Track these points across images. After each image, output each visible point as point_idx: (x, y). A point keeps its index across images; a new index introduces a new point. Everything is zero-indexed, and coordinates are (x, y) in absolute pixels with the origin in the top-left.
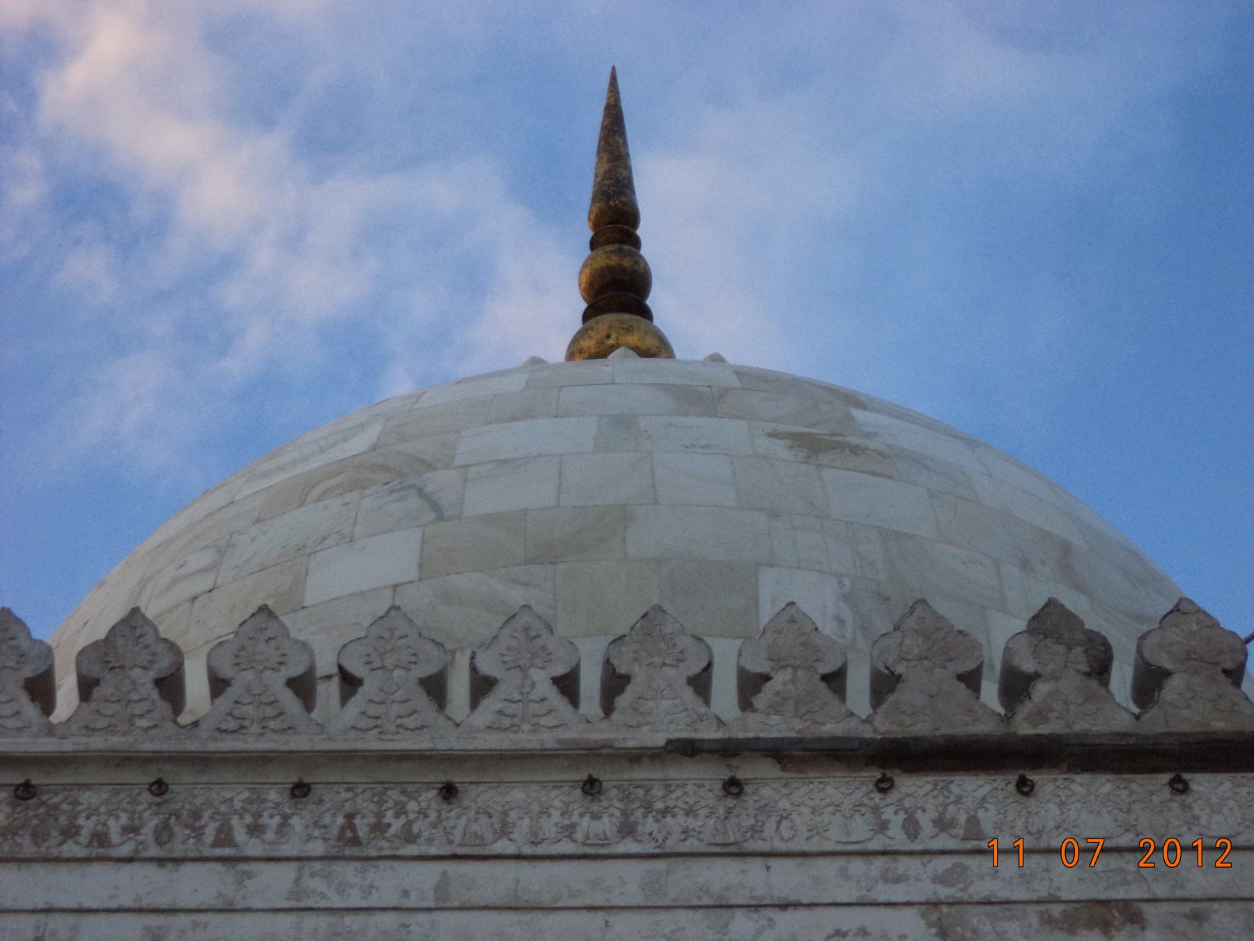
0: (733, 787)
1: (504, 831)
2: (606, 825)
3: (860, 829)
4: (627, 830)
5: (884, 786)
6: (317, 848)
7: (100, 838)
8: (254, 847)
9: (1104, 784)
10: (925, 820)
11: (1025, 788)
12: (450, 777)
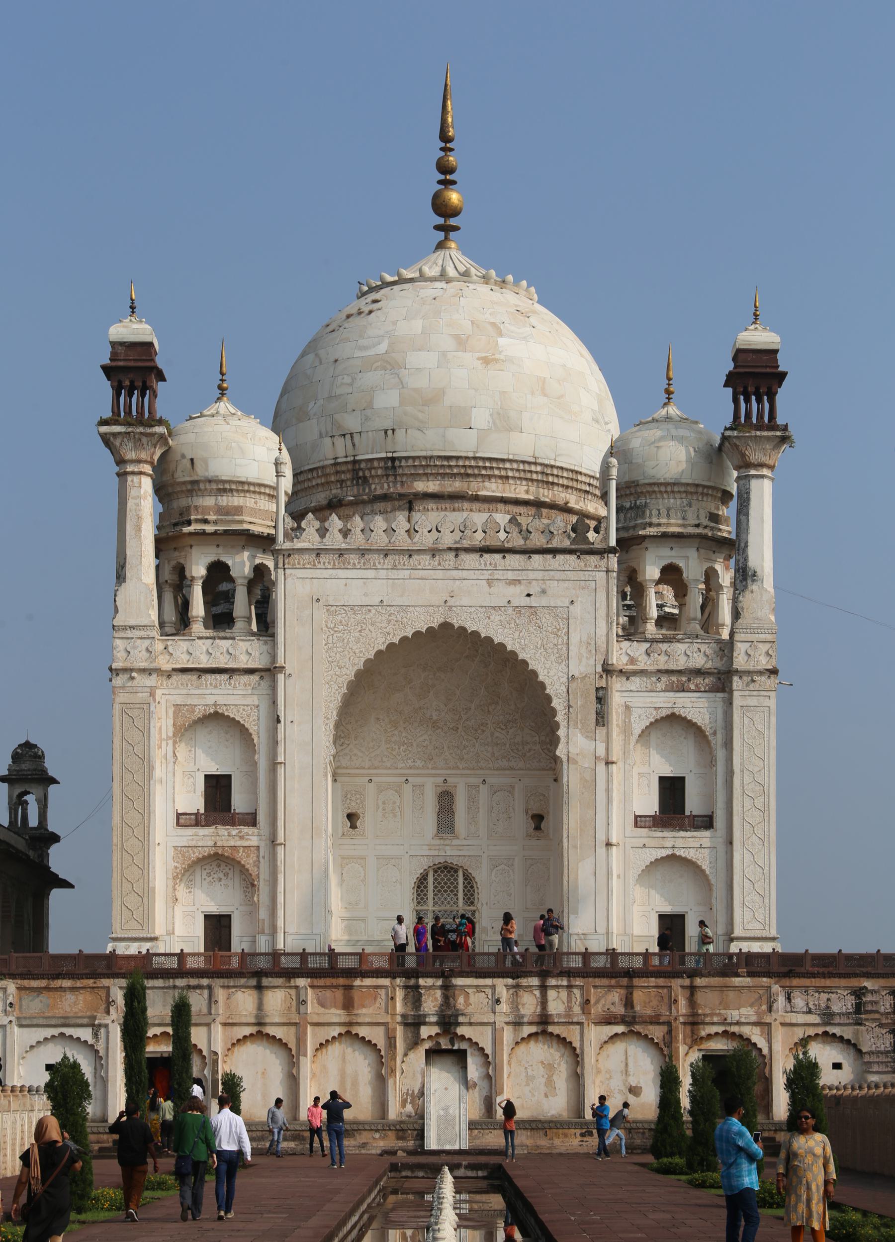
0: (457, 556)
1: (420, 564)
2: (436, 563)
3: (477, 566)
4: (439, 564)
5: (481, 556)
6: (390, 567)
7: (354, 564)
8: (379, 567)
9: (517, 556)
10: (488, 563)
11: (504, 557)
12: (410, 553)
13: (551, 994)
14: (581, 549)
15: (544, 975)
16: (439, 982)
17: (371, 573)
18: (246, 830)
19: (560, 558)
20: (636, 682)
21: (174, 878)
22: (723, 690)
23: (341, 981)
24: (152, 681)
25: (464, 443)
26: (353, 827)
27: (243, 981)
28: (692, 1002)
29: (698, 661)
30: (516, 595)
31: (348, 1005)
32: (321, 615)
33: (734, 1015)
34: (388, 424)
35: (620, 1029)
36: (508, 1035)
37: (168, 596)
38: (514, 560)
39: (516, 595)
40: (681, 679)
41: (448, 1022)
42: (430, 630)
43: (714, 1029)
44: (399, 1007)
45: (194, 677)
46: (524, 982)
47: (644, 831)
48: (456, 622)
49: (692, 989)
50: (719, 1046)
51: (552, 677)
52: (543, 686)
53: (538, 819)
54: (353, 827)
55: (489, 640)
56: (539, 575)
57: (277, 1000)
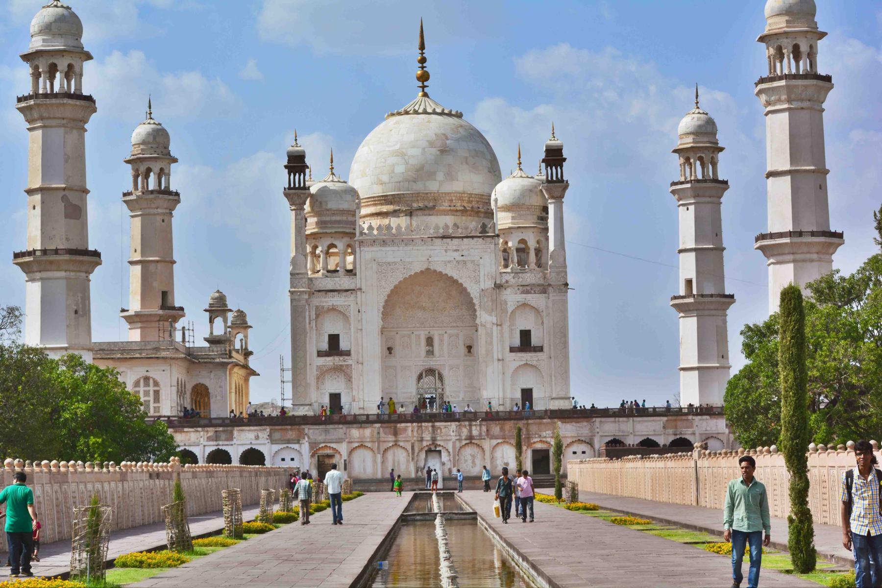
13: (474, 428)
14: (485, 232)
15: (470, 420)
16: (430, 424)
17: (396, 248)
18: (346, 357)
19: (475, 239)
20: (509, 291)
21: (318, 378)
22: (545, 293)
23: (392, 425)
24: (306, 297)
25: (433, 186)
26: (390, 353)
27: (355, 426)
28: (528, 430)
29: (533, 282)
30: (457, 256)
31: (395, 434)
32: (375, 266)
33: (544, 434)
34: (400, 179)
35: (500, 441)
36: (457, 443)
37: (309, 258)
38: (455, 241)
39: (457, 256)
40: (527, 289)
41: (434, 440)
42: (422, 272)
43: (536, 440)
44: (415, 434)
45: (323, 293)
46: (463, 423)
47: (513, 354)
48: (432, 268)
49: (528, 424)
50: (539, 446)
51: (474, 290)
52: (469, 294)
53: (469, 348)
54: (390, 353)
55: (446, 275)
56: (467, 247)
57: (368, 432)
